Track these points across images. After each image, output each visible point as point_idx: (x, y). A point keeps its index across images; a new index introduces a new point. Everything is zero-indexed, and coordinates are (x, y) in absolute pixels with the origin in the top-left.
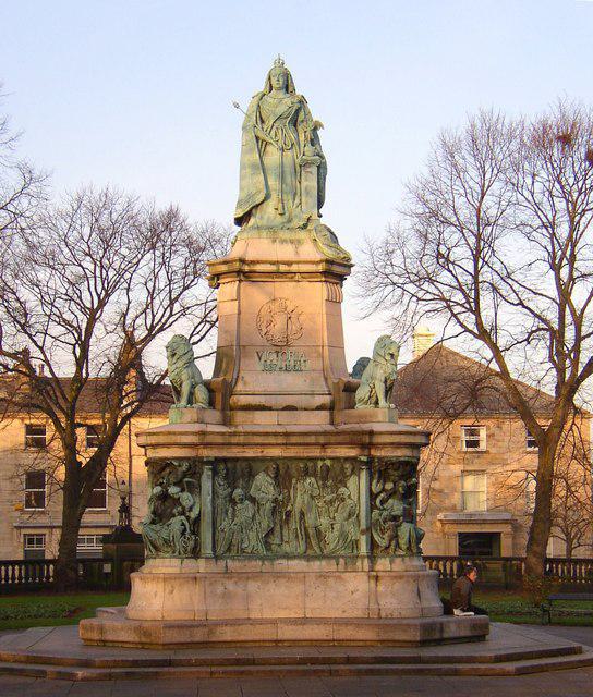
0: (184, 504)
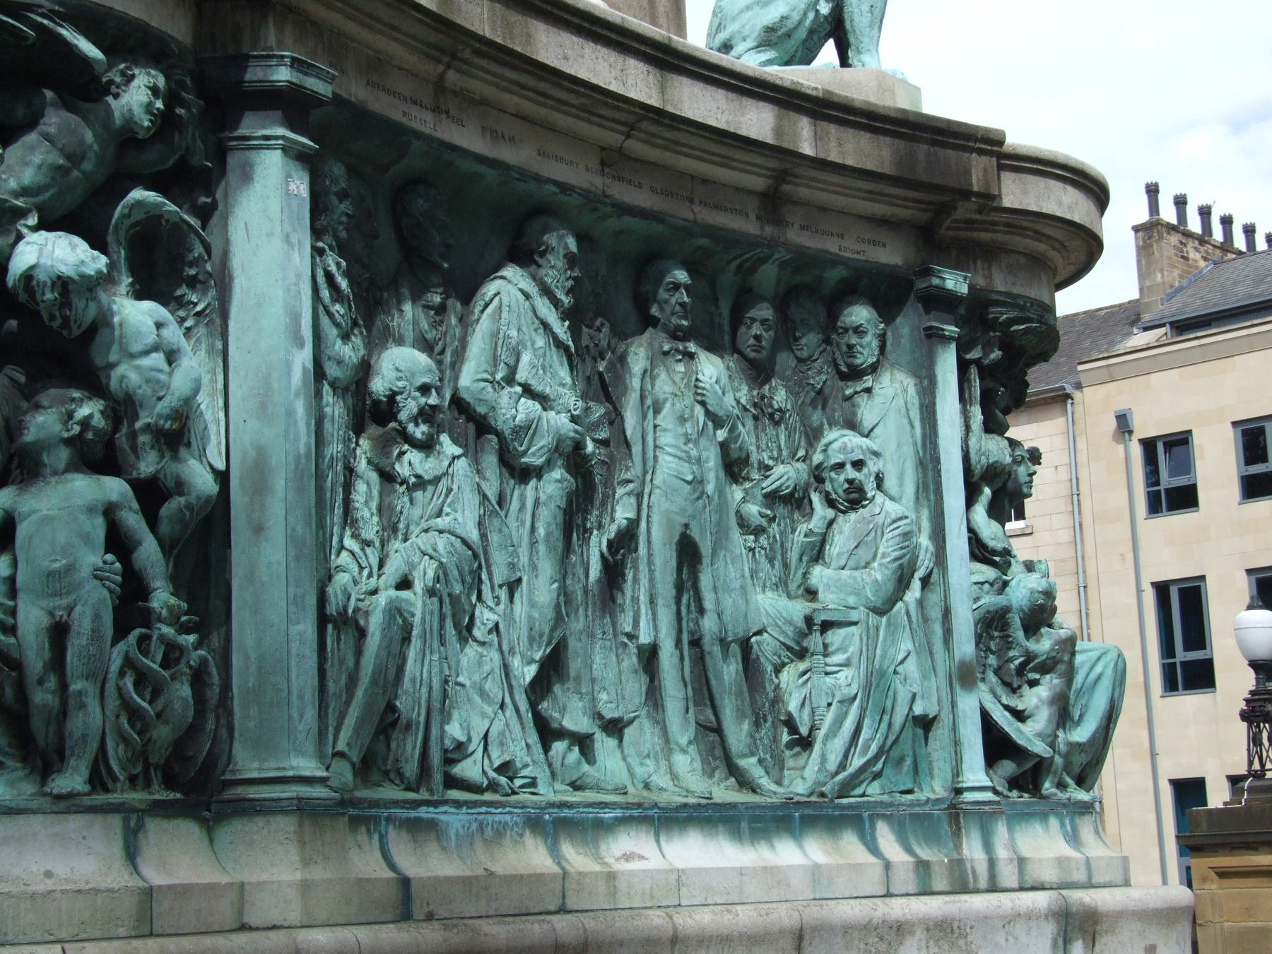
0: (126, 375)
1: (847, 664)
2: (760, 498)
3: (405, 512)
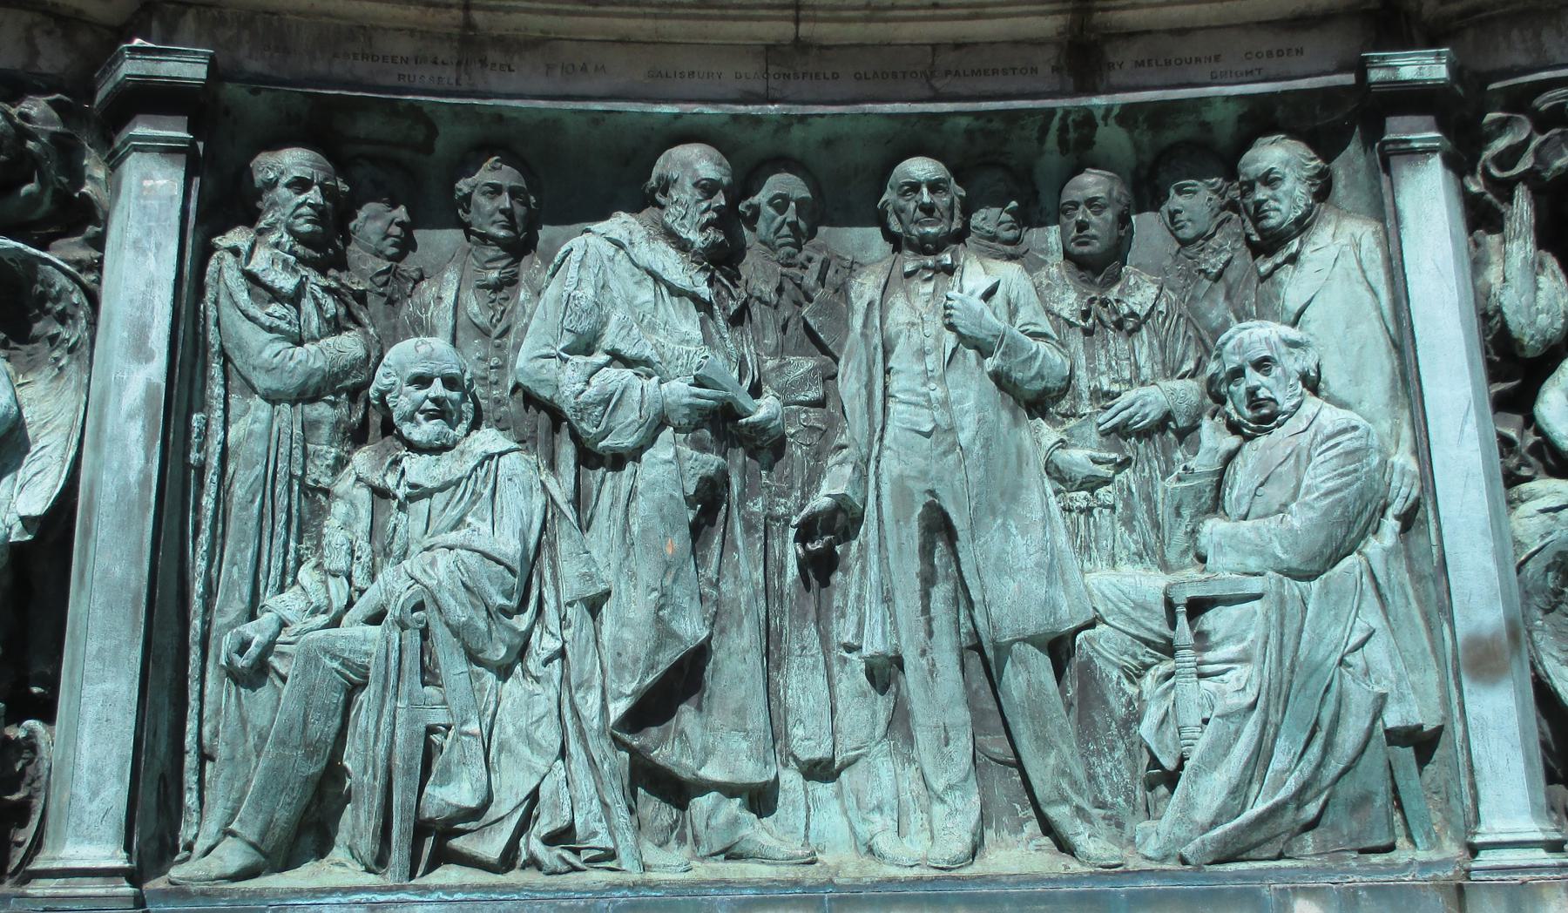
1: (1244, 659)
2: (1095, 437)
3: (400, 529)
